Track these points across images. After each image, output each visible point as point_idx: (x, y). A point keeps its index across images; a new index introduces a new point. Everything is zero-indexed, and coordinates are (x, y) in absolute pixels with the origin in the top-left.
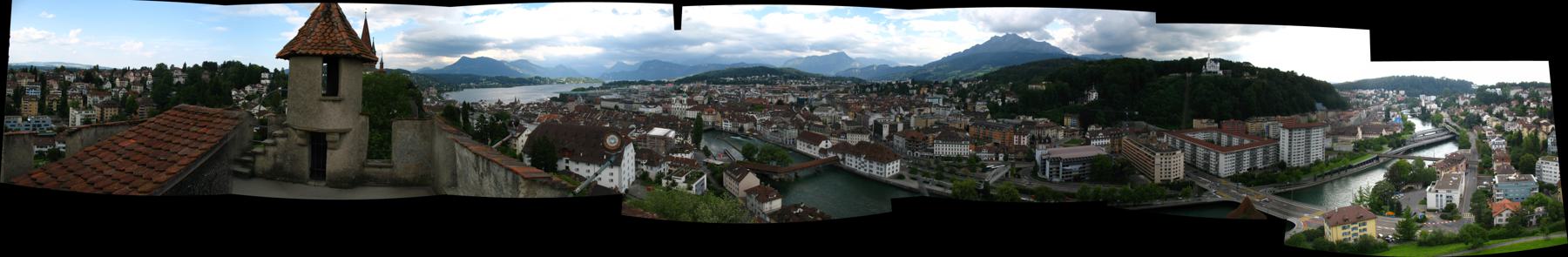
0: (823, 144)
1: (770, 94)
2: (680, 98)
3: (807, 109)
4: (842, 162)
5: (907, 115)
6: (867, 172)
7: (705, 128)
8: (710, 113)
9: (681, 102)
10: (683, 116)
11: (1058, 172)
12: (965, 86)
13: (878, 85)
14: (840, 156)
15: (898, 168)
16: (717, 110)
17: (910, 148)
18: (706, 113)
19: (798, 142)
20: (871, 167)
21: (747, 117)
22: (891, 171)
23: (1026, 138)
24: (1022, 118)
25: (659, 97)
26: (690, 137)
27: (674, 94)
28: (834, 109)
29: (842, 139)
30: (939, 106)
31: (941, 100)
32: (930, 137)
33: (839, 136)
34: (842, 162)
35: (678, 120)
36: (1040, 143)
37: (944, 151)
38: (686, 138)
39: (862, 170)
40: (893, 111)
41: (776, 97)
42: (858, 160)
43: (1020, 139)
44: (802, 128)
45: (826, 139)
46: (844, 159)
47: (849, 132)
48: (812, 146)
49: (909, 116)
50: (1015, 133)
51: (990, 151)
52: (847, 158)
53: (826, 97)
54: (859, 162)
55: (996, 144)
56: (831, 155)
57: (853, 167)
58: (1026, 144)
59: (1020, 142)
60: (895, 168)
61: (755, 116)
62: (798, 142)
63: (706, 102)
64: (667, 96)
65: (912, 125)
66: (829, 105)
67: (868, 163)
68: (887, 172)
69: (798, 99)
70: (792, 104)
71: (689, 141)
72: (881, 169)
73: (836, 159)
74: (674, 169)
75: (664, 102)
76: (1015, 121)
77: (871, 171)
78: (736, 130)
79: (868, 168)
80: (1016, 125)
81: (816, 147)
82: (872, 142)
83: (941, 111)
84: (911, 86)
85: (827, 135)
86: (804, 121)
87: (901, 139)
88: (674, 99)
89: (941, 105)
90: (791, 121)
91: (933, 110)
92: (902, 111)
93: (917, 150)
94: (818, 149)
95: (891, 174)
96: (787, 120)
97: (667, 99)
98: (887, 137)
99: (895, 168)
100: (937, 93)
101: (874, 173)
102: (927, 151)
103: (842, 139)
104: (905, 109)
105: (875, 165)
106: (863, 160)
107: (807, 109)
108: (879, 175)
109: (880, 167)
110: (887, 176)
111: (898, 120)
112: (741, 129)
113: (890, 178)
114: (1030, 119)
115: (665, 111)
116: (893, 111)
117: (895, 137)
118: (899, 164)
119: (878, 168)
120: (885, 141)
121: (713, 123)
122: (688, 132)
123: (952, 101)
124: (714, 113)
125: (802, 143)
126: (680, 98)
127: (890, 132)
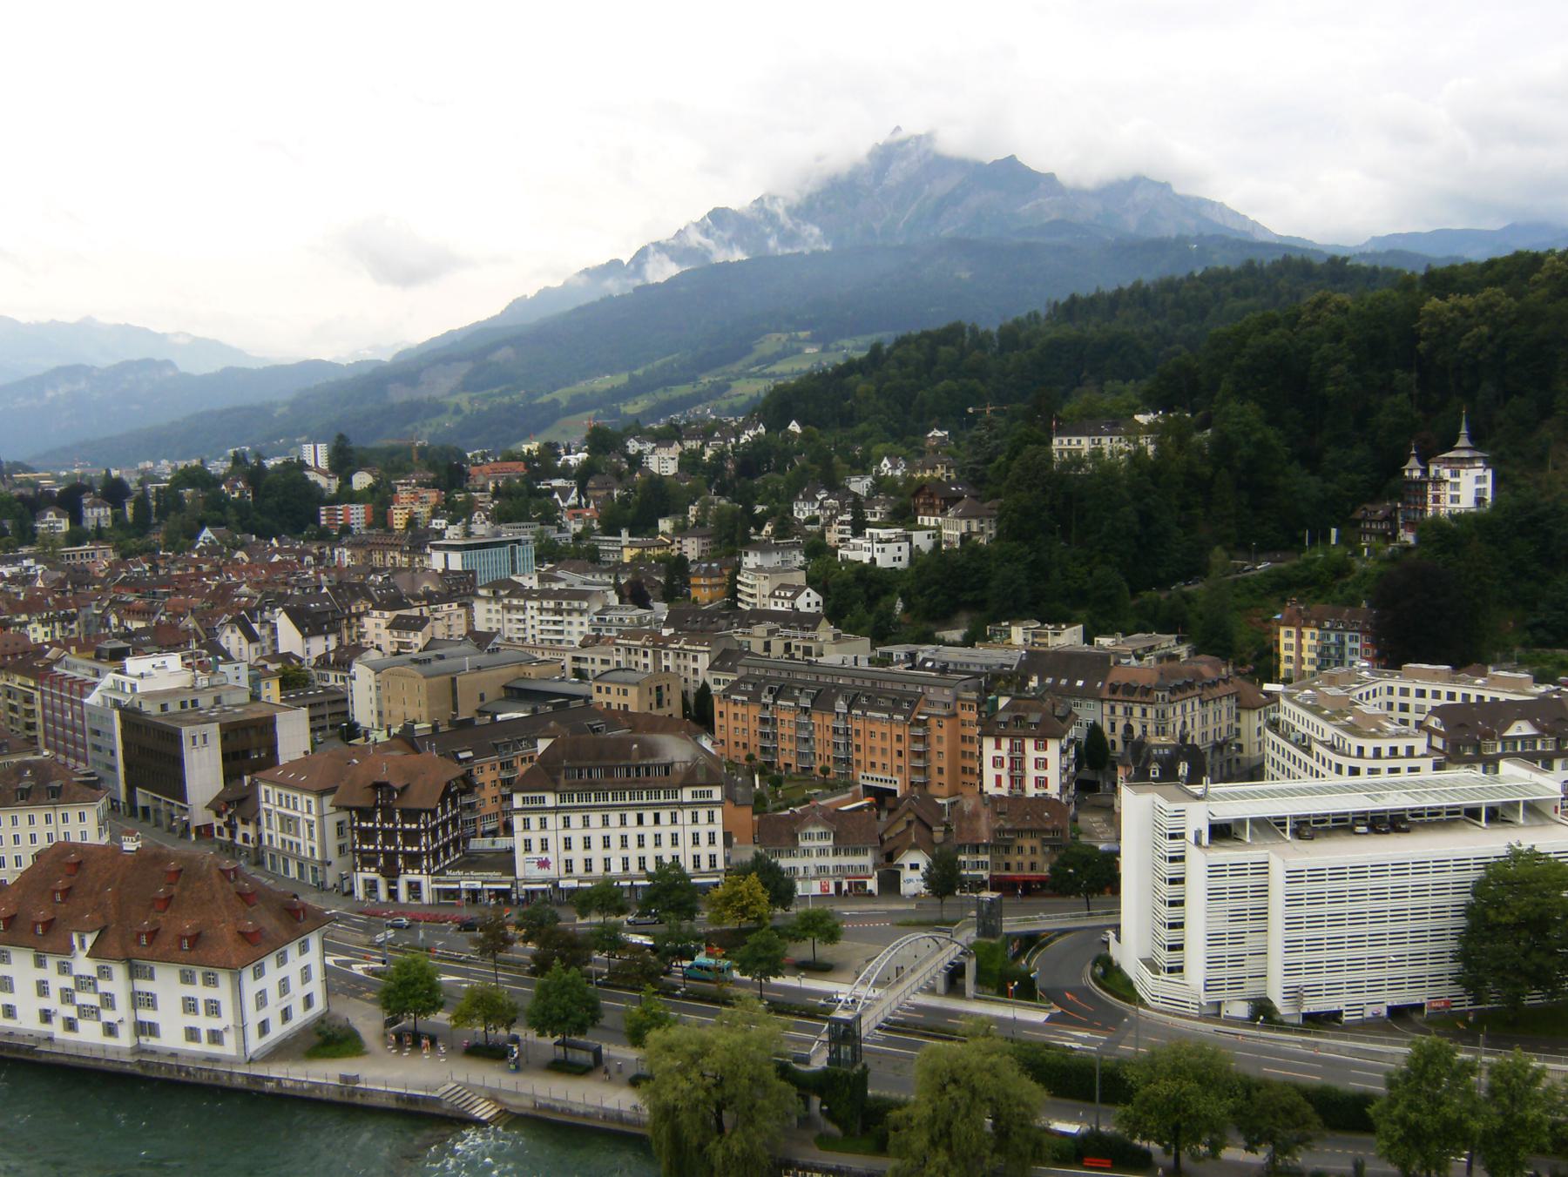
5: (323, 661)
11: (1262, 914)
12: (663, 462)
13: (114, 492)
15: (316, 987)
17: (368, 860)
20: (141, 1000)
22: (272, 1012)
23: (1054, 747)
24: (1018, 634)
30: (517, 590)
31: (527, 553)
32: (487, 775)
36: (1140, 777)
37: (578, 855)
39: (89, 1034)
40: (232, 639)
42: (50, 973)
43: (1017, 763)
49: (342, 661)
50: (990, 727)
51: (846, 835)
54: (58, 982)
55: (881, 796)
57: (27, 1022)
58: (1053, 790)
59: (1017, 780)
60: (298, 991)
65: (363, 711)
67: (118, 983)
68: (253, 1018)
72: (213, 1008)
76: (986, 655)
79: (122, 1012)
80: (994, 680)
82: (130, 845)
83: (533, 622)
84: (330, 485)
87: (305, 807)
89: (531, 582)
91: (485, 615)
92: (289, 637)
93: (413, 861)
95: (278, 1031)
98: (217, 806)
99: (298, 991)
100: (500, 517)
101: (171, 1038)
102: (472, 862)
104: (309, 624)
105: (166, 984)
106: (84, 965)
108: (203, 1047)
109: (200, 992)
110: (255, 1044)
111: (272, 691)
113: (281, 1051)
114: (1069, 638)
116: (232, 639)
117: (270, 797)
118: (314, 957)
119: (190, 1006)
120: (205, 831)
123: (590, 558)
127: (231, 775)
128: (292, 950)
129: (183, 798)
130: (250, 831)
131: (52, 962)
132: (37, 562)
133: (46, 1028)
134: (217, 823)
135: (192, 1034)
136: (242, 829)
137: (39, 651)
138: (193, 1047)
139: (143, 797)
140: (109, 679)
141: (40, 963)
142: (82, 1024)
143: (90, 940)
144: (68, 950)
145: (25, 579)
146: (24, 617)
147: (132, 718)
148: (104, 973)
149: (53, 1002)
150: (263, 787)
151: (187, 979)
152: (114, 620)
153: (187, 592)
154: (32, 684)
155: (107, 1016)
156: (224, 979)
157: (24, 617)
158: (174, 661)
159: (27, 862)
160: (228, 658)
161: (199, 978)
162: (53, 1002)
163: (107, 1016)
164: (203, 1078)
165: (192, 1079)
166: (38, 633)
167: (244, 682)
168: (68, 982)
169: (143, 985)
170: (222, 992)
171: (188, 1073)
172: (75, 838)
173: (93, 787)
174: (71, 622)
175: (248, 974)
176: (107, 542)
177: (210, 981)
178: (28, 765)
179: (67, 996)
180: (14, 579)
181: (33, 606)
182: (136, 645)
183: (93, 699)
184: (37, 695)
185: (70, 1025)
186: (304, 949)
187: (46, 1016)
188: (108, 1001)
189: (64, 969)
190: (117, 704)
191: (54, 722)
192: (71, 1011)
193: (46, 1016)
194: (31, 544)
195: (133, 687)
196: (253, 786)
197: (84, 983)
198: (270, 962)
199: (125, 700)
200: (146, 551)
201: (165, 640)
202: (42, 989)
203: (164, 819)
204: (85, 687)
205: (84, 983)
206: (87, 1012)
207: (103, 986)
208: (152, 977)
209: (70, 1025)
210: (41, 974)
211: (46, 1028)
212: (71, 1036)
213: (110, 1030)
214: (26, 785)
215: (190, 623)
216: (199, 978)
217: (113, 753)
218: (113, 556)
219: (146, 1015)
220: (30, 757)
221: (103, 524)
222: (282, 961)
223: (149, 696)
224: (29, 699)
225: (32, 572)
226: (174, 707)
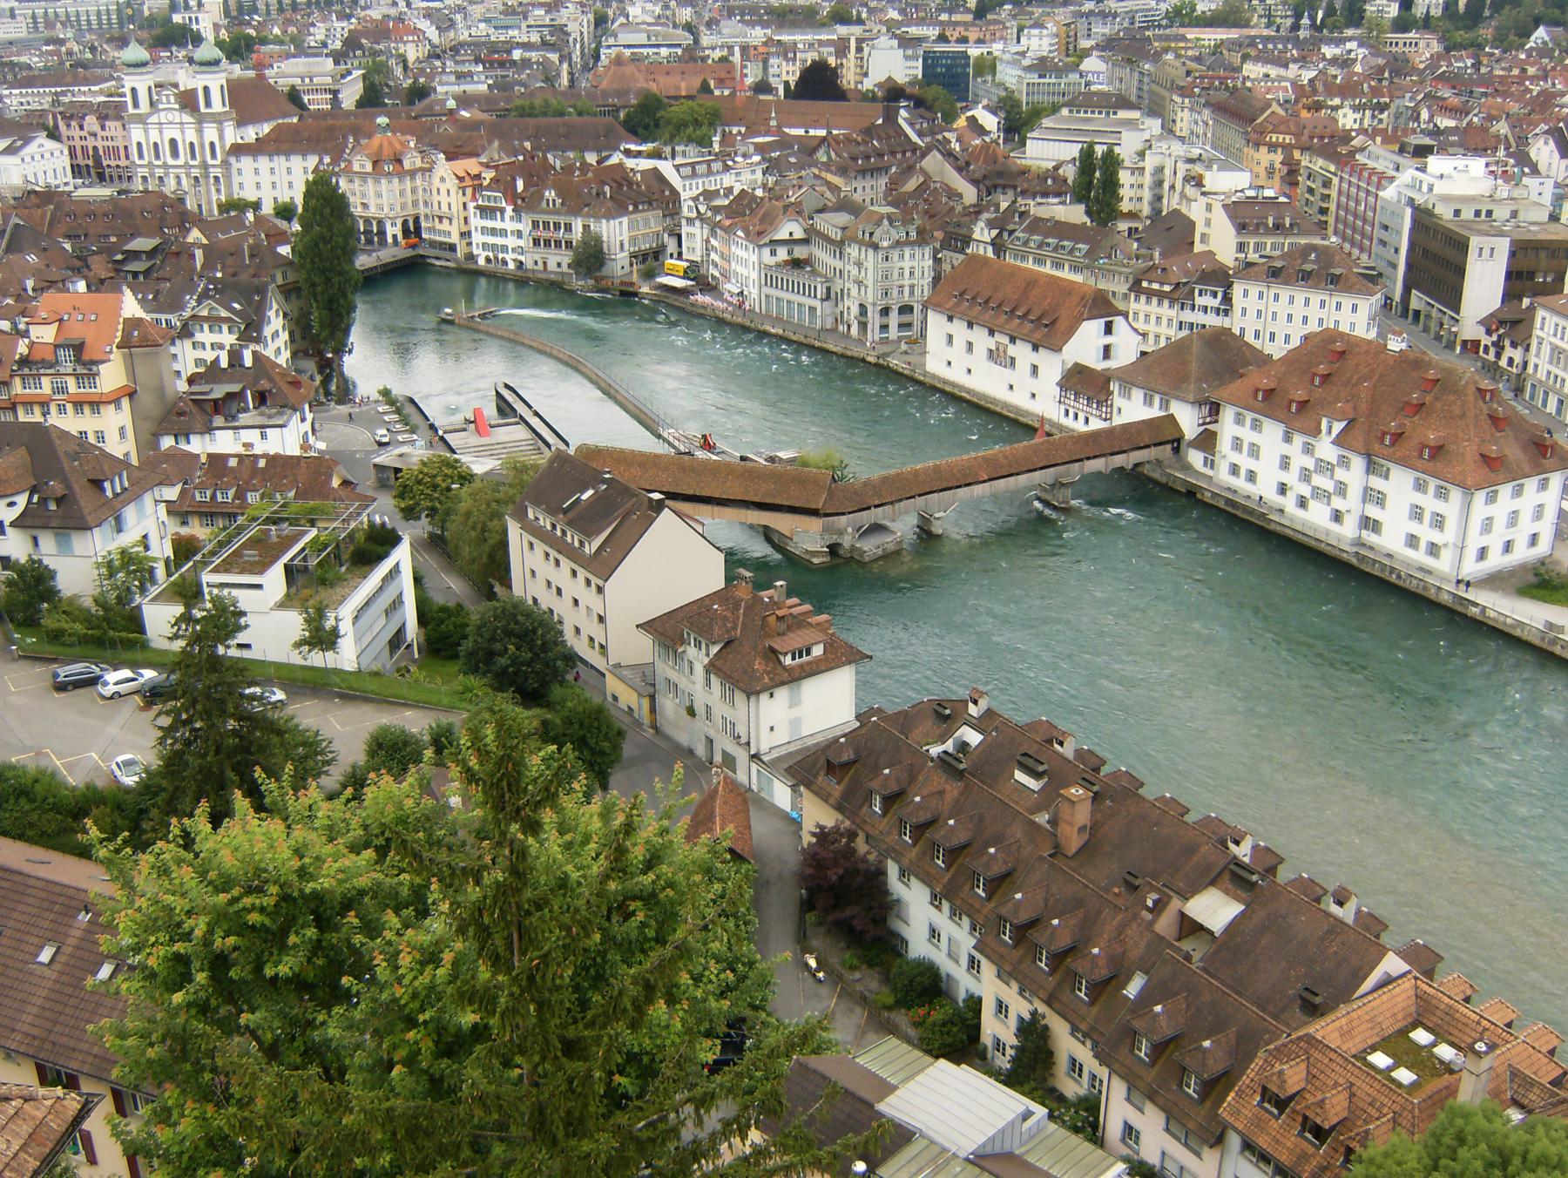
0: (1086, 343)
1: (757, 35)
2: (187, 79)
3: (990, 122)
4: (1195, 458)
6: (1348, 530)
7: (363, 261)
8: (388, 164)
9: (188, 101)
10: (217, 197)
14: (1188, 419)
16: (430, 142)
18: (362, 163)
19: (937, 325)
20: (1373, 496)
21: (621, 178)
25: (28, 79)
26: (275, 323)
27: (135, 52)
28: (1154, 126)
29: (1204, 314)
33: (1181, 296)
34: (1195, 458)
35: (185, 219)
38: (251, 330)
41: (787, 51)
44: (958, 240)
45: (1102, 307)
46: (1207, 441)
47: (1246, 269)
48: (1021, 351)
52: (1228, 428)
53: (1108, 45)
54: (1300, 460)
56: (1133, 409)
57: (1265, 489)
61: (666, 168)
62: (937, 325)
63: (351, 95)
64: (80, 71)
66: (1124, 103)
67: (1355, 473)
69: (930, 61)
70: (894, 93)
71: (276, 344)
72: (1439, 522)
73: (1164, 434)
74: (198, 530)
75: (75, 114)
77: (1369, 524)
78: (558, 261)
79: (1351, 504)
81: (1044, 358)
82: (1395, 345)
85: (1118, 286)
86: (969, 194)
88: (140, 82)
90: (893, 196)
94: (1052, 366)
96: (867, 191)
97: (93, 94)
98: (1489, 324)
101: (1391, 540)
103: (1204, 314)
105: (1399, 484)
106: (1326, 449)
107: (990, 122)
108: (1420, 556)
109: (1430, 503)
112: (591, 257)
115: (90, 167)
119: (1417, 513)
120: (1472, 347)
121: (412, 230)
122: (261, 291)
124: (412, 160)
125: (959, 328)
126: (187, 79)
128: (1531, 484)
129: (1457, 310)
130: (1517, 355)
131: (1299, 440)
132: (1360, 46)
133: (1280, 500)
134: (1486, 340)
135: (1412, 541)
136: (1508, 352)
137: (1346, 137)
138: (1410, 553)
139: (1417, 300)
140: (1408, 174)
141: (1288, 439)
142: (1312, 504)
143: (1338, 427)
144: (1316, 432)
145: (1345, 62)
146: (1337, 101)
147: (1423, 219)
148: (1344, 462)
149: (1291, 478)
150: (1540, 313)
151: (1420, 487)
152: (1425, 115)
153: (1505, 95)
154: (1332, 168)
155: (1337, 503)
156: (1456, 494)
157: (1337, 101)
158: (1477, 165)
159: (1295, 342)
160: (1535, 171)
161: (1431, 489)
162: (1291, 478)
163: (1337, 503)
164: (1412, 585)
165: (1401, 583)
166: (1347, 119)
167: (1547, 199)
168: (1309, 463)
169: (1376, 482)
170: (1451, 508)
171: (1399, 577)
172: (1344, 328)
173: (1373, 279)
174: (1382, 112)
175: (1480, 496)
176: (1433, 32)
177: (1442, 494)
178: (1314, 248)
179: (1305, 476)
180: (1334, 61)
181: (1348, 90)
182: (1439, 143)
183: (1389, 193)
184: (1336, 181)
185: (1302, 503)
186: (1543, 486)
187: (1283, 489)
188: (1341, 489)
189: (1308, 450)
190: (1411, 201)
191: (1347, 210)
192: (1305, 490)
193: (1283, 489)
194: (1357, 25)
195: (1431, 189)
196: (1531, 309)
197: (1324, 467)
198: (1505, 491)
199: (1420, 199)
200: (1472, 45)
201: (1475, 142)
202: (1285, 463)
203: (1434, 326)
204: (1383, 179)
205: (1324, 467)
206: (1319, 493)
207: (1340, 474)
208: (1387, 478)
209: (1302, 503)
210: (1286, 449)
211: (1280, 500)
212: (1300, 513)
213: (1337, 517)
214: (1308, 267)
215: (1502, 128)
216: (1431, 489)
217: (1397, 251)
218: (1436, 47)
219: (1373, 511)
220: (1317, 241)
221: (1433, 13)
222: (1518, 492)
223: (1446, 199)
224: (1327, 184)
225: (1353, 55)
226: (1468, 214)
